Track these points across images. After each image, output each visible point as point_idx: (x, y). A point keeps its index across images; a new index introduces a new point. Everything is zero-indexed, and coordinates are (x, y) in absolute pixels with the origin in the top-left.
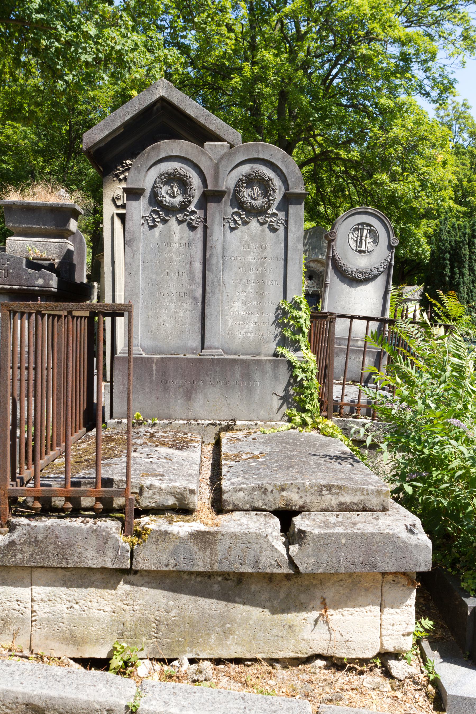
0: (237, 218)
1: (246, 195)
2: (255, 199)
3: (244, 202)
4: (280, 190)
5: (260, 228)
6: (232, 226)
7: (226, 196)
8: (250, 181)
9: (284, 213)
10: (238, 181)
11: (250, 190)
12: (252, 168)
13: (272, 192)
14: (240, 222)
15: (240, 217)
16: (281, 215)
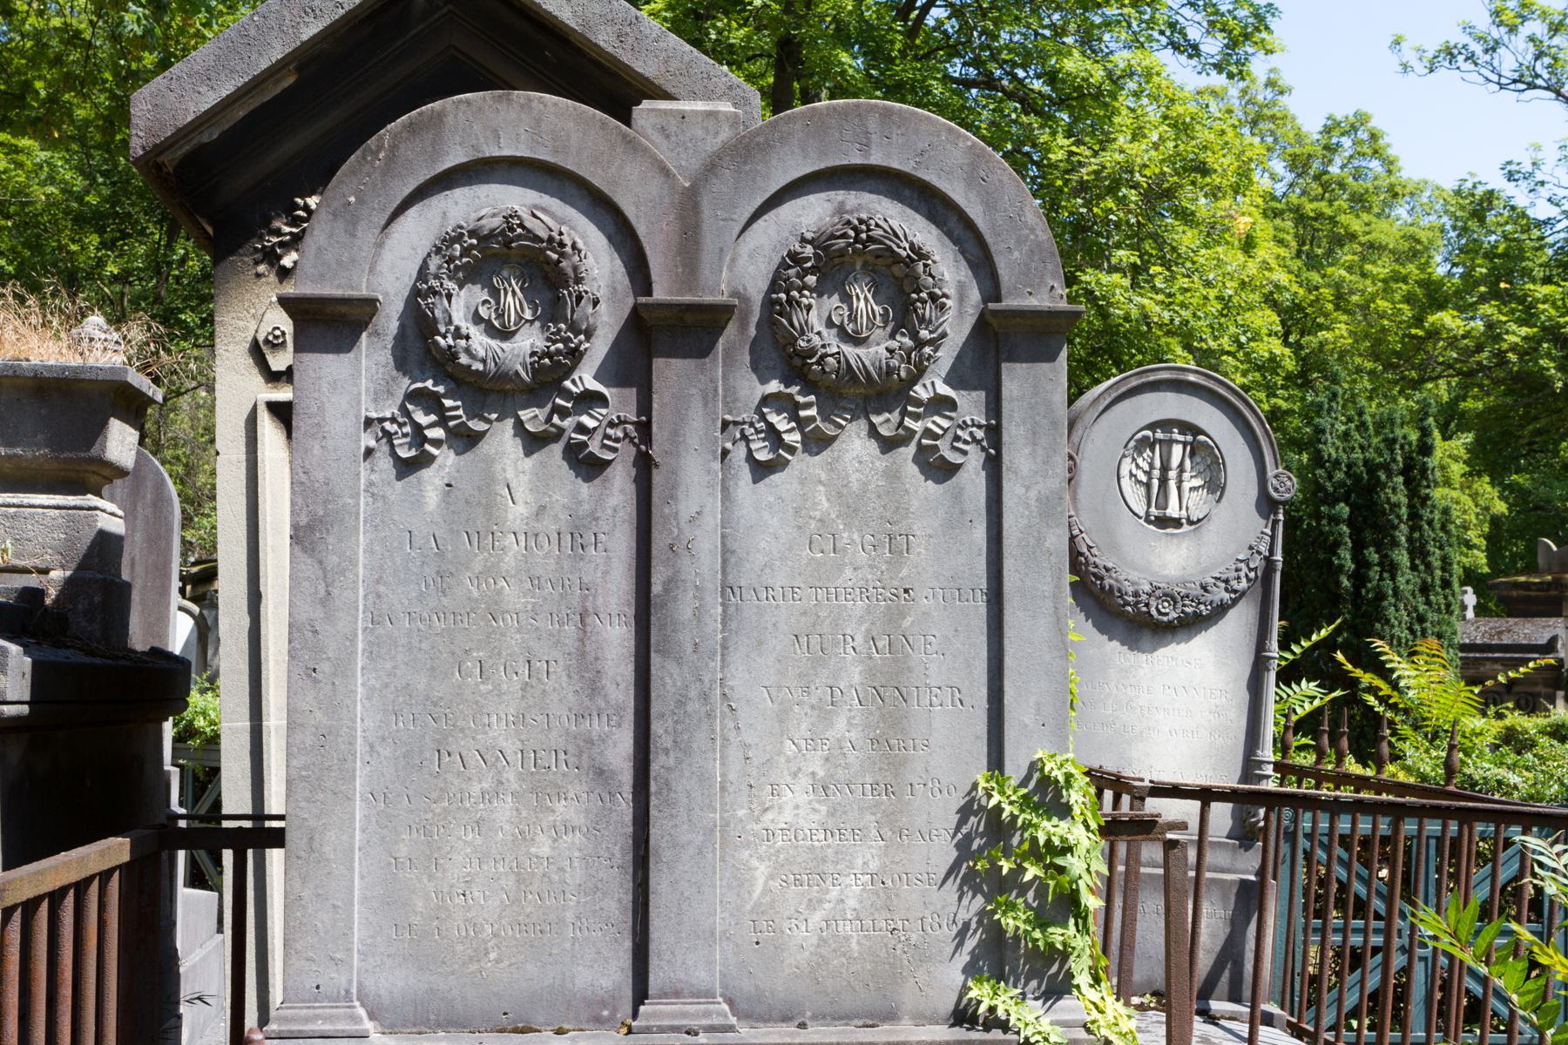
0: (780, 422)
1: (817, 320)
2: (857, 340)
3: (812, 352)
4: (962, 298)
5: (882, 462)
6: (762, 456)
7: (731, 330)
8: (833, 261)
9: (980, 396)
10: (783, 265)
11: (835, 301)
12: (840, 210)
13: (928, 311)
14: (793, 438)
15: (794, 417)
16: (971, 406)
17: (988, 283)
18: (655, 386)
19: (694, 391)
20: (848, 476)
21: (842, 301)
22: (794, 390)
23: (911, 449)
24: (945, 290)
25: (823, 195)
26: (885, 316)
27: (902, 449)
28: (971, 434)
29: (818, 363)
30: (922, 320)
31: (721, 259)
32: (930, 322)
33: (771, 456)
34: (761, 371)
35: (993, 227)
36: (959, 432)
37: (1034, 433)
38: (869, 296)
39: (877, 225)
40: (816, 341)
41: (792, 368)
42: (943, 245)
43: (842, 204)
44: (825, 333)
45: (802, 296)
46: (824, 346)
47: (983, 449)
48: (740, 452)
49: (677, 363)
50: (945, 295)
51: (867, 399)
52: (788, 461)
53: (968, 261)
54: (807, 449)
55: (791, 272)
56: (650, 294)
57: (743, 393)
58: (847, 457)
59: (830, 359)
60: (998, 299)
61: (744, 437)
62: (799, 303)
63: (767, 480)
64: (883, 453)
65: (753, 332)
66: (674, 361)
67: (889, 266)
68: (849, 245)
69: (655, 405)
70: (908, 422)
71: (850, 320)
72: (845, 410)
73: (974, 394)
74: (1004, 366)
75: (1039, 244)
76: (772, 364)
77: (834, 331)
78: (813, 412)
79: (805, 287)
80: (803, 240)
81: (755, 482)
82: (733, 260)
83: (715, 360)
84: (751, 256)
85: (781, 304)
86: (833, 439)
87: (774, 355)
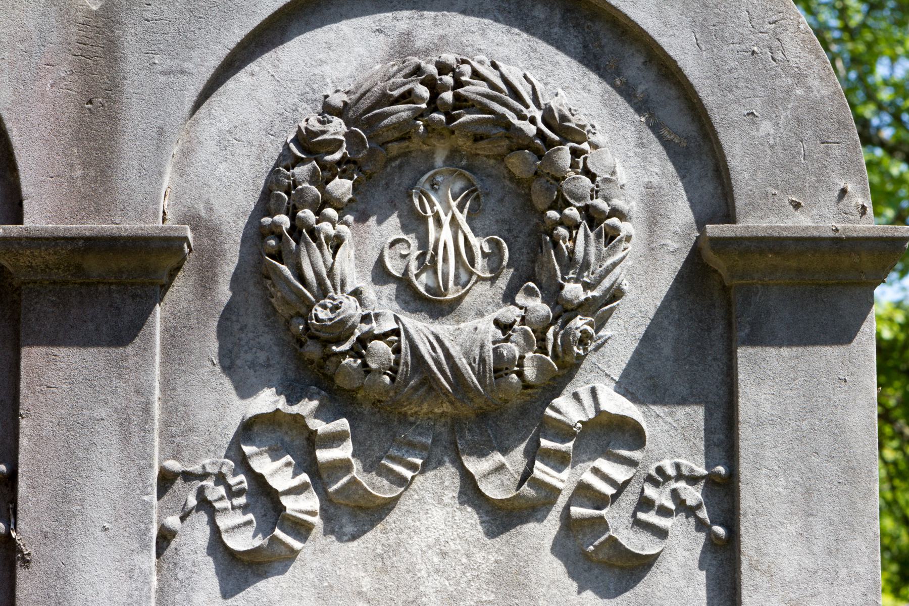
0: (279, 473)
1: (355, 266)
2: (436, 306)
3: (341, 331)
4: (654, 219)
5: (490, 553)
6: (242, 541)
7: (182, 288)
8: (377, 151)
9: (694, 416)
10: (288, 160)
11: (392, 227)
12: (403, 46)
13: (582, 243)
14: (304, 505)
15: (306, 463)
16: (674, 436)
17: (709, 187)
18: (25, 403)
19: (103, 412)
20: (417, 580)
21: (405, 228)
22: (305, 407)
23: (548, 528)
24: (618, 202)
25: (368, 21)
26: (493, 257)
27: (530, 527)
28: (675, 494)
29: (355, 352)
30: (568, 262)
31: (160, 147)
32: (586, 265)
33: (259, 542)
34: (240, 372)
35: (717, 72)
36: (650, 492)
37: (808, 491)
38: (462, 218)
39: (476, 74)
40: (351, 308)
41: (302, 363)
42: (614, 113)
43: (407, 36)
44: (370, 292)
45: (322, 217)
46: (366, 319)
47: (701, 525)
48: (196, 534)
49: (70, 357)
50: (616, 212)
51: (456, 425)
52: (294, 553)
53: (666, 144)
54: (332, 527)
55: (301, 171)
56: (19, 220)
57: (203, 416)
58: (417, 543)
59: (379, 346)
60: (729, 217)
61: (205, 504)
62: (314, 233)
63: (251, 592)
64: (492, 533)
65: (224, 293)
66: (62, 352)
67: (501, 158)
68: (420, 115)
69: (24, 441)
70: (541, 471)
71: (422, 267)
72: (412, 447)
73: (681, 412)
74: (742, 352)
75: (814, 106)
76: (262, 356)
77: (390, 289)
78: (345, 451)
79: (328, 201)
80: (328, 109)
81: (226, 594)
82: (186, 153)
83: (147, 347)
84: (222, 144)
85: (279, 237)
86: (388, 506)
87: (267, 339)
